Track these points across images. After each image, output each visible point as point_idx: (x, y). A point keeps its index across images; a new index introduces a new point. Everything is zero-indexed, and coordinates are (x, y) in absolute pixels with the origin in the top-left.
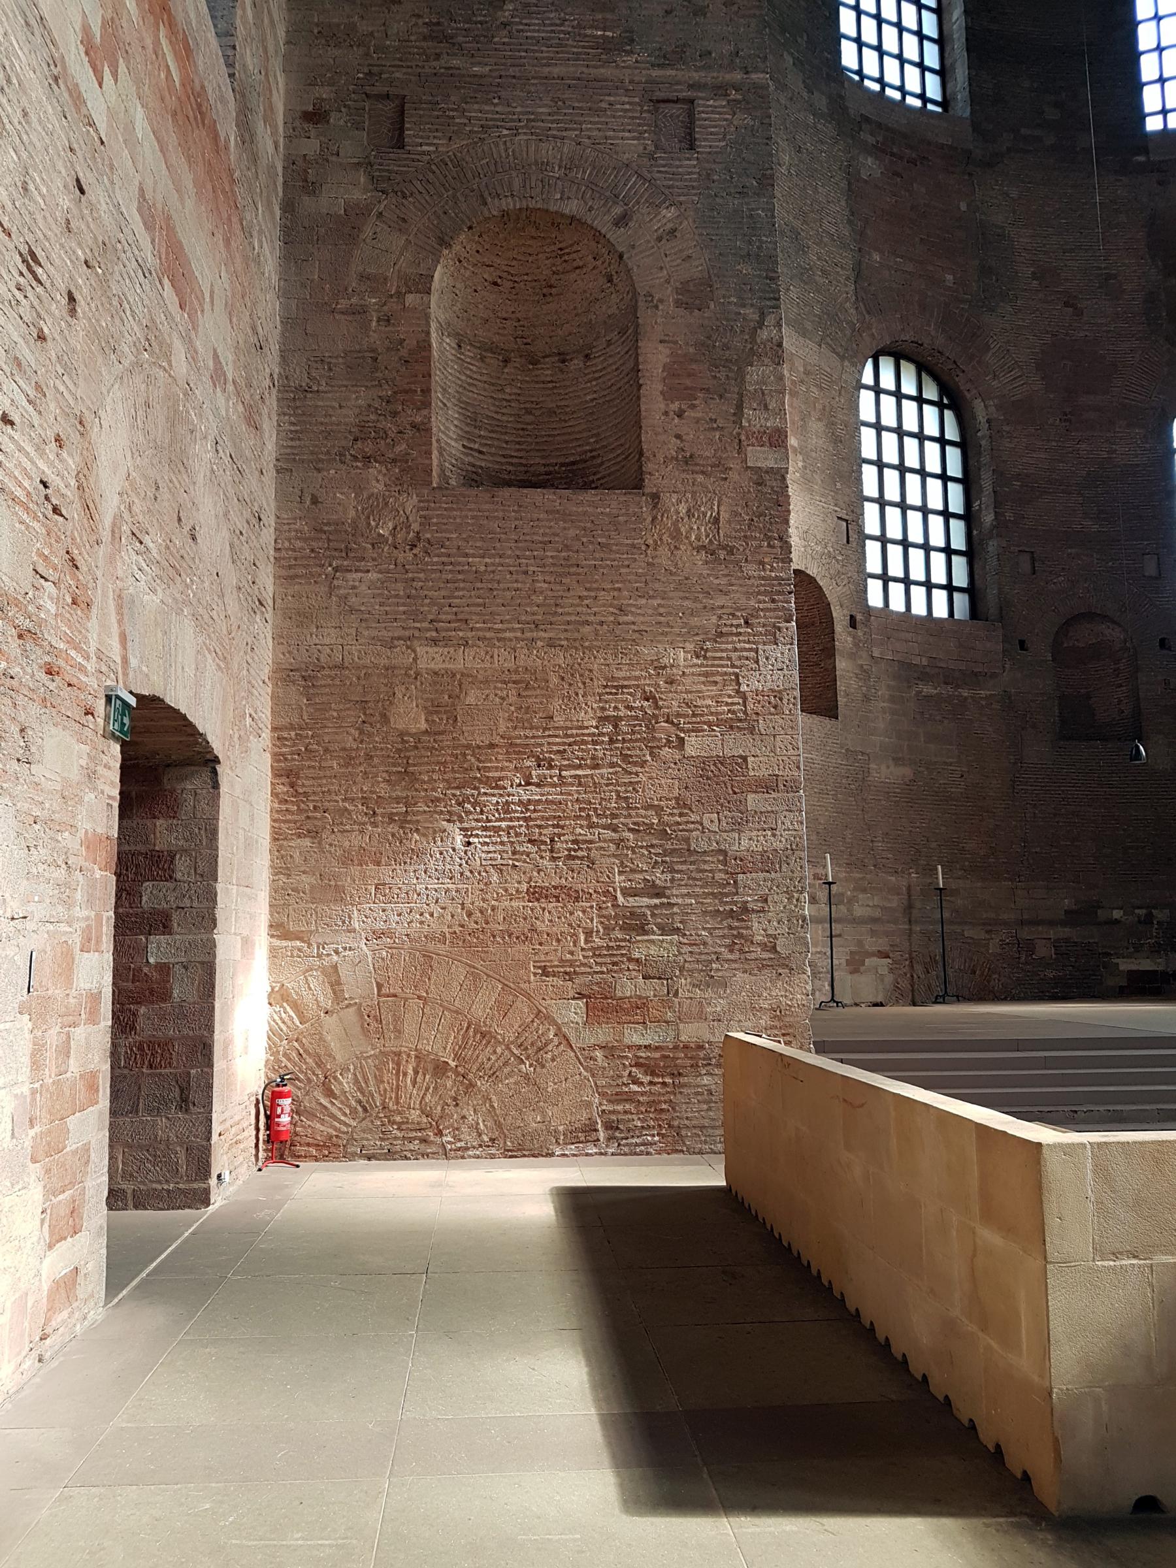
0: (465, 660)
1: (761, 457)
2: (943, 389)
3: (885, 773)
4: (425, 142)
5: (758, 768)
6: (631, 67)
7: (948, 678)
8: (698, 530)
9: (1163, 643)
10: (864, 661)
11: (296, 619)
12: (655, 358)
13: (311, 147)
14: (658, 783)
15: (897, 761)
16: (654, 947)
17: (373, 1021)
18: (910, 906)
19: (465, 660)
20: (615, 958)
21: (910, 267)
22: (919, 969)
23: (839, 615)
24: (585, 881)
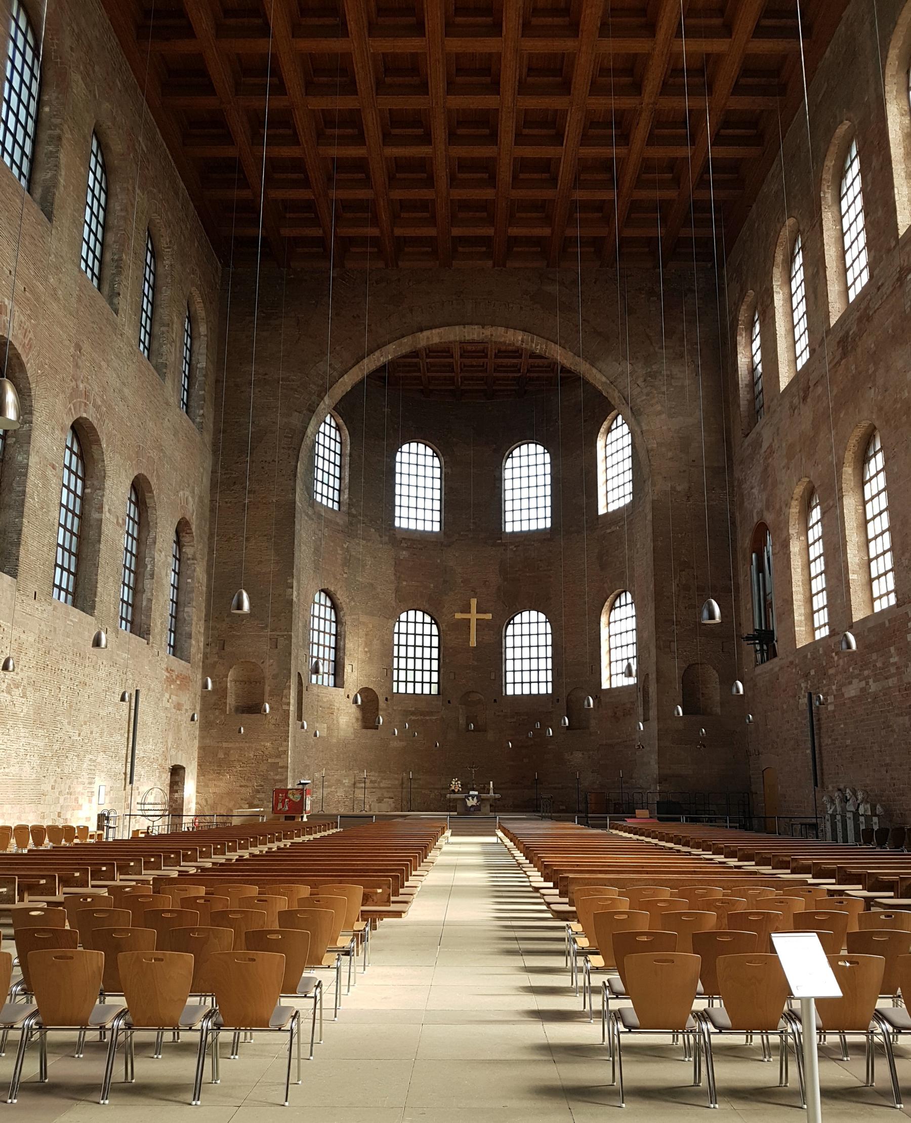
0: (230, 745)
1: (285, 707)
2: (432, 618)
3: (395, 744)
4: (228, 649)
5: (280, 764)
6: (268, 632)
7: (422, 714)
8: (273, 721)
9: (495, 701)
10: (390, 711)
11: (202, 738)
12: (267, 689)
13: (208, 650)
14: (263, 767)
15: (401, 740)
16: (262, 796)
17: (212, 808)
18: (402, 783)
19: (230, 745)
20: (253, 797)
22: (405, 803)
23: (381, 699)
24: (249, 784)
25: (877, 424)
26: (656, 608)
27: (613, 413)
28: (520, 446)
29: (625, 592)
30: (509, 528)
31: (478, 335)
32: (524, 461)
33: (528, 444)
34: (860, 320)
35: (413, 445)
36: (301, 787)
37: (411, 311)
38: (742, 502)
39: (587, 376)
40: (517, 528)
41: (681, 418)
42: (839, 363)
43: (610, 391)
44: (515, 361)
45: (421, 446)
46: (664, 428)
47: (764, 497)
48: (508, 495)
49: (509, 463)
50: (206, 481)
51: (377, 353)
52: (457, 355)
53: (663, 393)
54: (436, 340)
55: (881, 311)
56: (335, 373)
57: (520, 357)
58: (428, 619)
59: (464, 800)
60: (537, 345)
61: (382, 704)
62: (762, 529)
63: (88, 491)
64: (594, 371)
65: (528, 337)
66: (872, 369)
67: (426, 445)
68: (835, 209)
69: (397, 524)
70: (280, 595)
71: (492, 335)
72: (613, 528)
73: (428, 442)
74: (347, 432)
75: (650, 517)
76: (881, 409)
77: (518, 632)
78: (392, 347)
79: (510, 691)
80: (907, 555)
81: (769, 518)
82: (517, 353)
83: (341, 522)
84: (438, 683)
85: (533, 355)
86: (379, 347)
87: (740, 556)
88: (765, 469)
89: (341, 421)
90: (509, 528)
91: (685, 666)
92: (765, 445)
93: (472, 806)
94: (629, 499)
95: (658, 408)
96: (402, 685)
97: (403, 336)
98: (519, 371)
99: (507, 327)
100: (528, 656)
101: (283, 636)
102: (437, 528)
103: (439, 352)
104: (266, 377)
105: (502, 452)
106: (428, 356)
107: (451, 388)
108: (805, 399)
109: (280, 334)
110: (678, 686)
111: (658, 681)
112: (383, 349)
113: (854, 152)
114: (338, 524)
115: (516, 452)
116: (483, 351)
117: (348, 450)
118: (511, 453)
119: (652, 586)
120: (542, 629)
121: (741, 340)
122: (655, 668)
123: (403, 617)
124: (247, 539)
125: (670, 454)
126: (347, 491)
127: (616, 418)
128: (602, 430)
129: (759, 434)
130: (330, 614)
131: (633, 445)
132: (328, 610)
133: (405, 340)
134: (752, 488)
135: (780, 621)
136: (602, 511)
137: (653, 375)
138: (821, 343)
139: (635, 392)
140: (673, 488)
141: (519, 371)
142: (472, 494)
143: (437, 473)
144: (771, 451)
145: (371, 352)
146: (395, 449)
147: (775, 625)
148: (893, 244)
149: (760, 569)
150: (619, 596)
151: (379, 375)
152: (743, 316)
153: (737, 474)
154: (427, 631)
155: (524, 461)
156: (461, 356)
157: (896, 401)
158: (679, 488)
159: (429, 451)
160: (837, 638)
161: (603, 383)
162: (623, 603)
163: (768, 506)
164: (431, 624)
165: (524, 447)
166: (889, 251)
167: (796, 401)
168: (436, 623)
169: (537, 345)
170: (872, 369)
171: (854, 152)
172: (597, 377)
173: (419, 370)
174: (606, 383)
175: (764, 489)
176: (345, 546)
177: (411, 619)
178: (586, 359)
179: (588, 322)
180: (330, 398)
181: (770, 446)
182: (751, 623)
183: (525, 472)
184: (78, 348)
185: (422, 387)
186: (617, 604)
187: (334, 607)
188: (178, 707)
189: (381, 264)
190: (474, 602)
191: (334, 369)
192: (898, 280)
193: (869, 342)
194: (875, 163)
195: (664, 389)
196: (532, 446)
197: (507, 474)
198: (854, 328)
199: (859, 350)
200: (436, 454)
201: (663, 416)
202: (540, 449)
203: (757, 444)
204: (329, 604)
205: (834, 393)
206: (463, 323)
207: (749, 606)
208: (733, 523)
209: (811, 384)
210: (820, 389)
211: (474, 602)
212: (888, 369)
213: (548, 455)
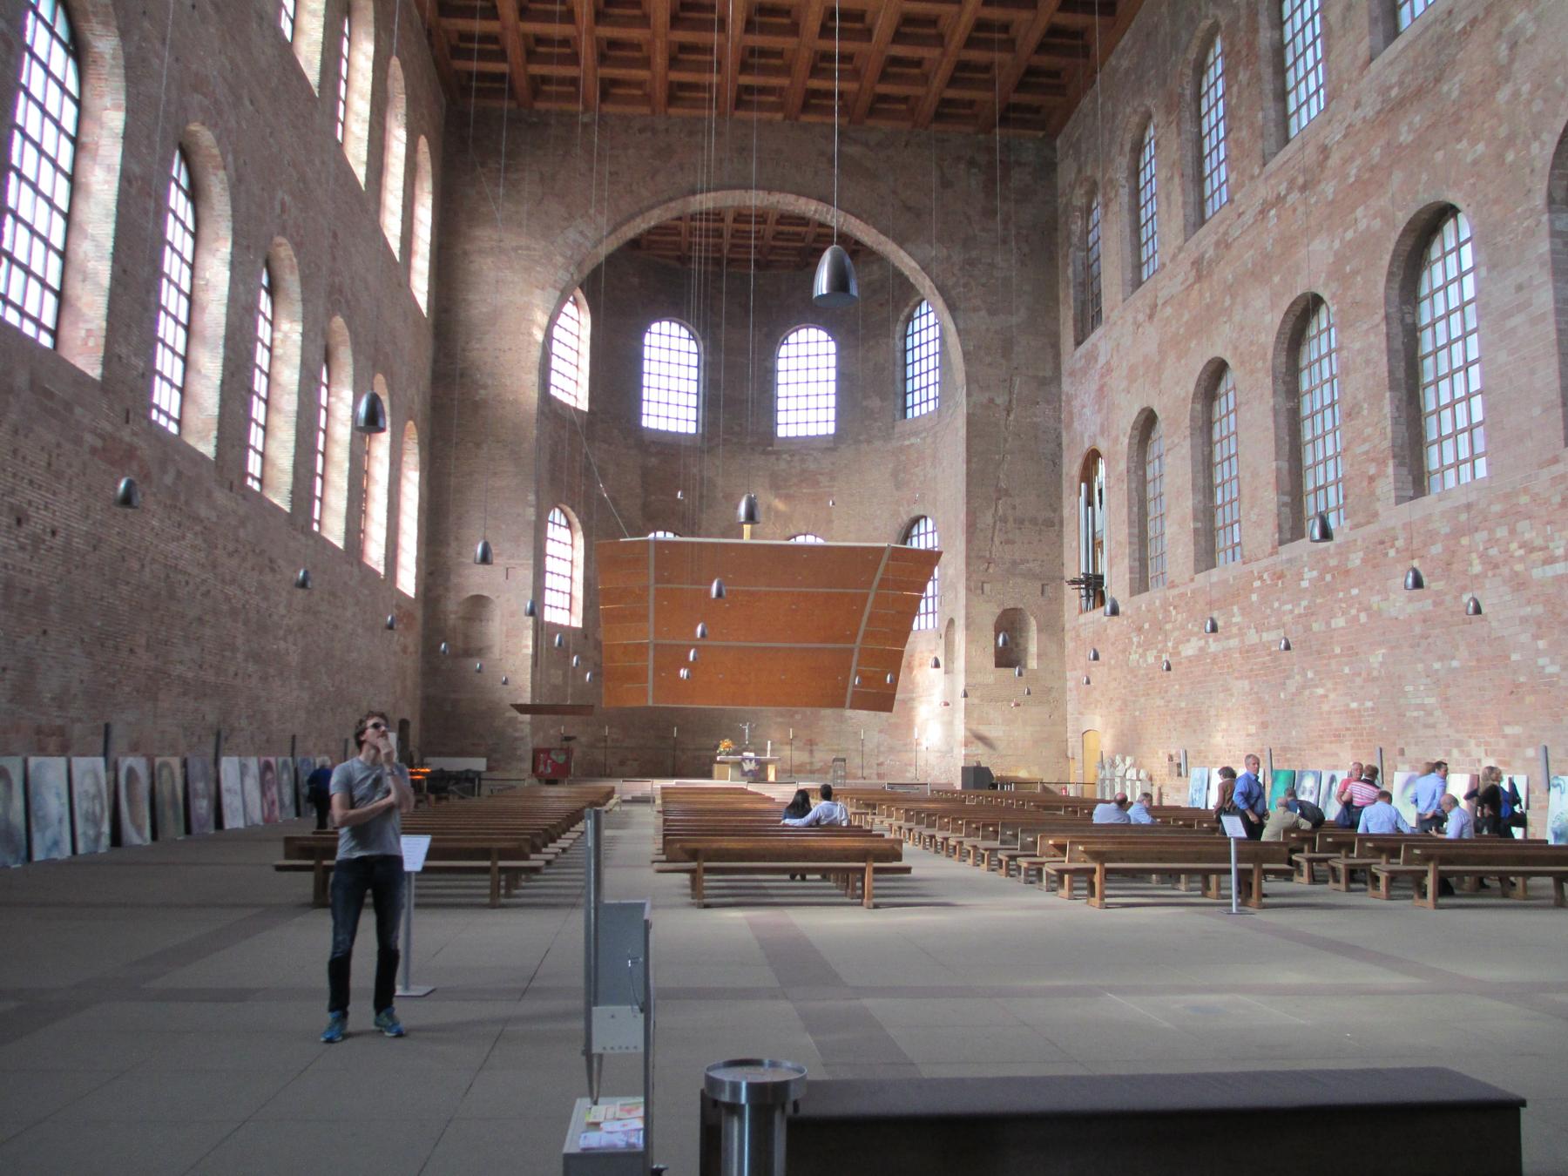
25: (1230, 362)
26: (969, 541)
30: (781, 432)
32: (803, 350)
34: (1217, 244)
35: (665, 324)
36: (565, 744)
38: (1069, 425)
39: (892, 257)
42: (1192, 285)
44: (799, 229)
45: (675, 326)
47: (1098, 419)
48: (781, 391)
49: (783, 351)
50: (428, 373)
51: (639, 220)
54: (711, 205)
55: (1241, 241)
62: (1093, 457)
63: (333, 400)
64: (902, 253)
65: (823, 207)
66: (1228, 302)
68: (1193, 108)
69: (644, 424)
72: (913, 440)
75: (963, 432)
76: (1236, 348)
80: (1256, 510)
81: (1102, 446)
82: (802, 220)
85: (821, 225)
87: (1065, 485)
88: (1101, 388)
91: (998, 611)
92: (1102, 360)
95: (978, 302)
97: (671, 199)
98: (803, 240)
99: (799, 194)
102: (692, 429)
108: (1151, 317)
111: (967, 627)
113: (1218, 49)
115: (792, 338)
119: (962, 516)
121: (1077, 227)
122: (963, 612)
124: (478, 445)
125: (988, 359)
128: (902, 318)
129: (1095, 346)
130: (564, 534)
131: (942, 339)
133: (672, 205)
134: (1083, 407)
135: (1111, 566)
137: (971, 263)
138: (1174, 258)
139: (950, 283)
140: (992, 400)
143: (694, 360)
144: (1108, 369)
145: (631, 217)
146: (643, 329)
147: (1103, 568)
148: (1257, 171)
149: (1090, 503)
151: (634, 243)
152: (1079, 200)
153: (1066, 385)
155: (803, 350)
156: (735, 220)
157: (1251, 343)
158: (999, 401)
159: (685, 333)
160: (1175, 592)
161: (911, 268)
162: (922, 530)
163: (1104, 430)
165: (803, 332)
166: (1252, 178)
167: (1141, 317)
170: (1228, 302)
171: (1218, 49)
172: (905, 262)
173: (679, 234)
175: (1100, 410)
178: (894, 239)
180: (580, 272)
181: (1108, 362)
182: (1076, 566)
184: (335, 236)
186: (915, 532)
187: (569, 526)
188: (405, 650)
189: (646, 110)
191: (586, 237)
192: (1262, 212)
193: (1226, 273)
194: (1243, 76)
195: (984, 280)
197: (781, 364)
198: (1210, 253)
199: (1215, 277)
200: (692, 337)
202: (823, 335)
203: (1092, 357)
204: (564, 522)
205: (1186, 317)
207: (1075, 544)
208: (1060, 445)
209: (1160, 302)
210: (1169, 311)
212: (1245, 307)
213: (832, 347)
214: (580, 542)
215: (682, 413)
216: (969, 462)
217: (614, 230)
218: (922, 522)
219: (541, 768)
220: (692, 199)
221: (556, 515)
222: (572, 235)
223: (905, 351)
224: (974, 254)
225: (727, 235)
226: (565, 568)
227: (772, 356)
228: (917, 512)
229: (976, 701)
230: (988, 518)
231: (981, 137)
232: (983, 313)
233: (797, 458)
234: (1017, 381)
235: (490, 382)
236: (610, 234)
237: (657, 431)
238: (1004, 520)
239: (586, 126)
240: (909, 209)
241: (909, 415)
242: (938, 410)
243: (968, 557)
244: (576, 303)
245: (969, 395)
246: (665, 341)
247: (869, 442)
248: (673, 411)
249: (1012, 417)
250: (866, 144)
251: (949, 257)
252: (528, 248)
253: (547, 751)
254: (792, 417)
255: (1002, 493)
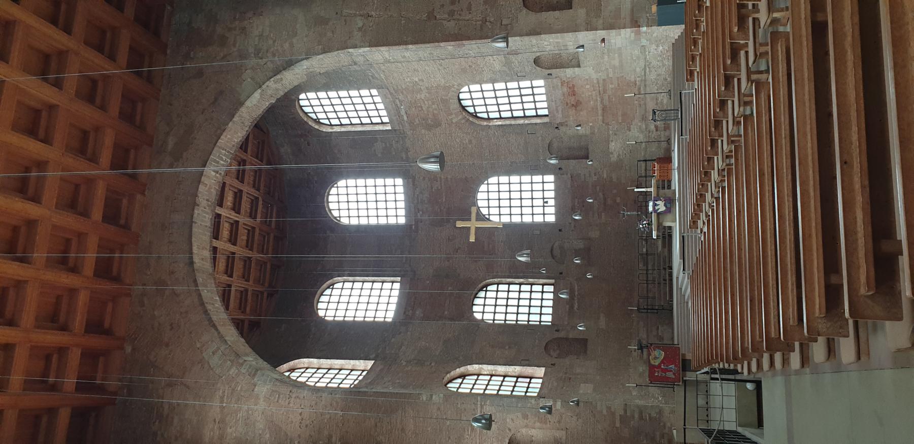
2: (481, 290)
3: (602, 323)
9: (560, 230)
21: (448, 302)
23: (557, 335)
26: (469, 39)
27: (301, 114)
28: (330, 210)
29: (460, 100)
30: (402, 221)
31: (207, 213)
32: (344, 206)
33: (328, 202)
37: (173, 273)
40: (402, 212)
41: (298, 26)
43: (269, 92)
45: (323, 299)
46: (305, 39)
48: (373, 221)
51: (209, 307)
52: (232, 248)
53: (274, 42)
56: (222, 348)
57: (241, 191)
58: (482, 294)
59: (659, 214)
60: (222, 159)
61: (562, 334)
64: (248, 103)
67: (322, 295)
69: (390, 320)
70: (439, 409)
71: (208, 200)
72: (403, 112)
73: (319, 292)
74: (296, 361)
77: (496, 211)
78: (205, 294)
79: (551, 219)
83: (381, 367)
84: (543, 285)
86: (202, 304)
89: (285, 366)
90: (402, 221)
91: (525, 11)
93: (665, 205)
94: (374, 92)
95: (286, 46)
96: (544, 318)
97: (195, 281)
98: (257, 198)
99: (199, 182)
100: (519, 200)
101: (482, 406)
103: (227, 266)
104: (217, 421)
105: (334, 226)
106: (231, 276)
107: (269, 266)
109: (178, 404)
110: (545, 15)
112: (205, 300)
114: (381, 370)
115: (335, 213)
116: (232, 224)
117: (315, 362)
118: (335, 218)
120: (493, 188)
122: (526, 38)
123: (478, 316)
125: (329, 34)
126: (352, 362)
127: (306, 113)
128: (317, 127)
132: (465, 381)
136: (389, 128)
139: (270, 65)
140: (360, 29)
141: (257, 198)
142: (369, 253)
145: (206, 312)
150: (463, 108)
154: (494, 294)
156: (234, 244)
158: (360, 24)
162: (469, 103)
164: (486, 291)
165: (332, 206)
168: (486, 286)
169: (222, 159)
174: (261, 95)
176: (404, 363)
177: (480, 309)
178: (237, 109)
179: (204, 110)
183: (353, 205)
185: (265, 295)
186: (471, 110)
187: (463, 376)
190: (460, 224)
191: (218, 348)
195: (271, 42)
196: (331, 198)
197: (354, 222)
201: (294, 40)
204: (460, 380)
206: (190, 223)
211: (460, 224)
214: (476, 367)
215: (385, 293)
216: (406, 43)
217: (214, 326)
218: (464, 103)
219: (670, 375)
220: (196, 266)
221: (453, 386)
222: (215, 361)
223: (341, 125)
224: (251, 50)
225: (249, 254)
226: (497, 380)
227: (347, 228)
228: (455, 105)
229: (601, 21)
230: (450, 25)
231: (168, 52)
232: (294, 40)
233: (420, 207)
234: (346, 11)
235: (326, 433)
236: (217, 330)
237: (397, 312)
238: (451, 13)
239: (133, 349)
240: (216, 99)
241: (386, 120)
242: (378, 88)
243: (481, 38)
244: (292, 370)
245: (355, 47)
246: (332, 306)
247: (407, 151)
248: (384, 300)
249: (373, 13)
250: (168, 134)
251: (253, 68)
252: (222, 398)
253: (652, 368)
254: (392, 212)
255: (431, 16)
